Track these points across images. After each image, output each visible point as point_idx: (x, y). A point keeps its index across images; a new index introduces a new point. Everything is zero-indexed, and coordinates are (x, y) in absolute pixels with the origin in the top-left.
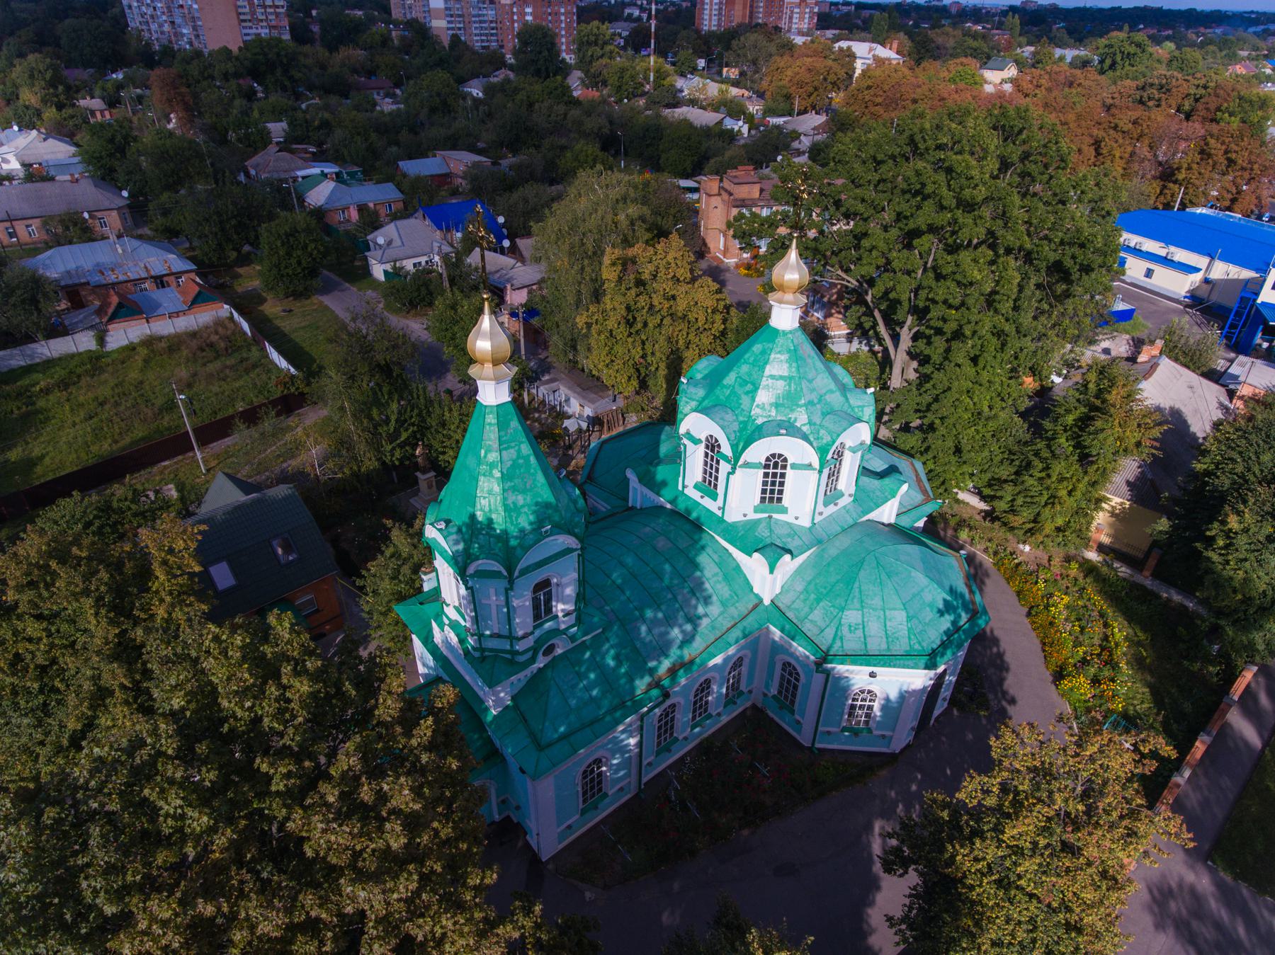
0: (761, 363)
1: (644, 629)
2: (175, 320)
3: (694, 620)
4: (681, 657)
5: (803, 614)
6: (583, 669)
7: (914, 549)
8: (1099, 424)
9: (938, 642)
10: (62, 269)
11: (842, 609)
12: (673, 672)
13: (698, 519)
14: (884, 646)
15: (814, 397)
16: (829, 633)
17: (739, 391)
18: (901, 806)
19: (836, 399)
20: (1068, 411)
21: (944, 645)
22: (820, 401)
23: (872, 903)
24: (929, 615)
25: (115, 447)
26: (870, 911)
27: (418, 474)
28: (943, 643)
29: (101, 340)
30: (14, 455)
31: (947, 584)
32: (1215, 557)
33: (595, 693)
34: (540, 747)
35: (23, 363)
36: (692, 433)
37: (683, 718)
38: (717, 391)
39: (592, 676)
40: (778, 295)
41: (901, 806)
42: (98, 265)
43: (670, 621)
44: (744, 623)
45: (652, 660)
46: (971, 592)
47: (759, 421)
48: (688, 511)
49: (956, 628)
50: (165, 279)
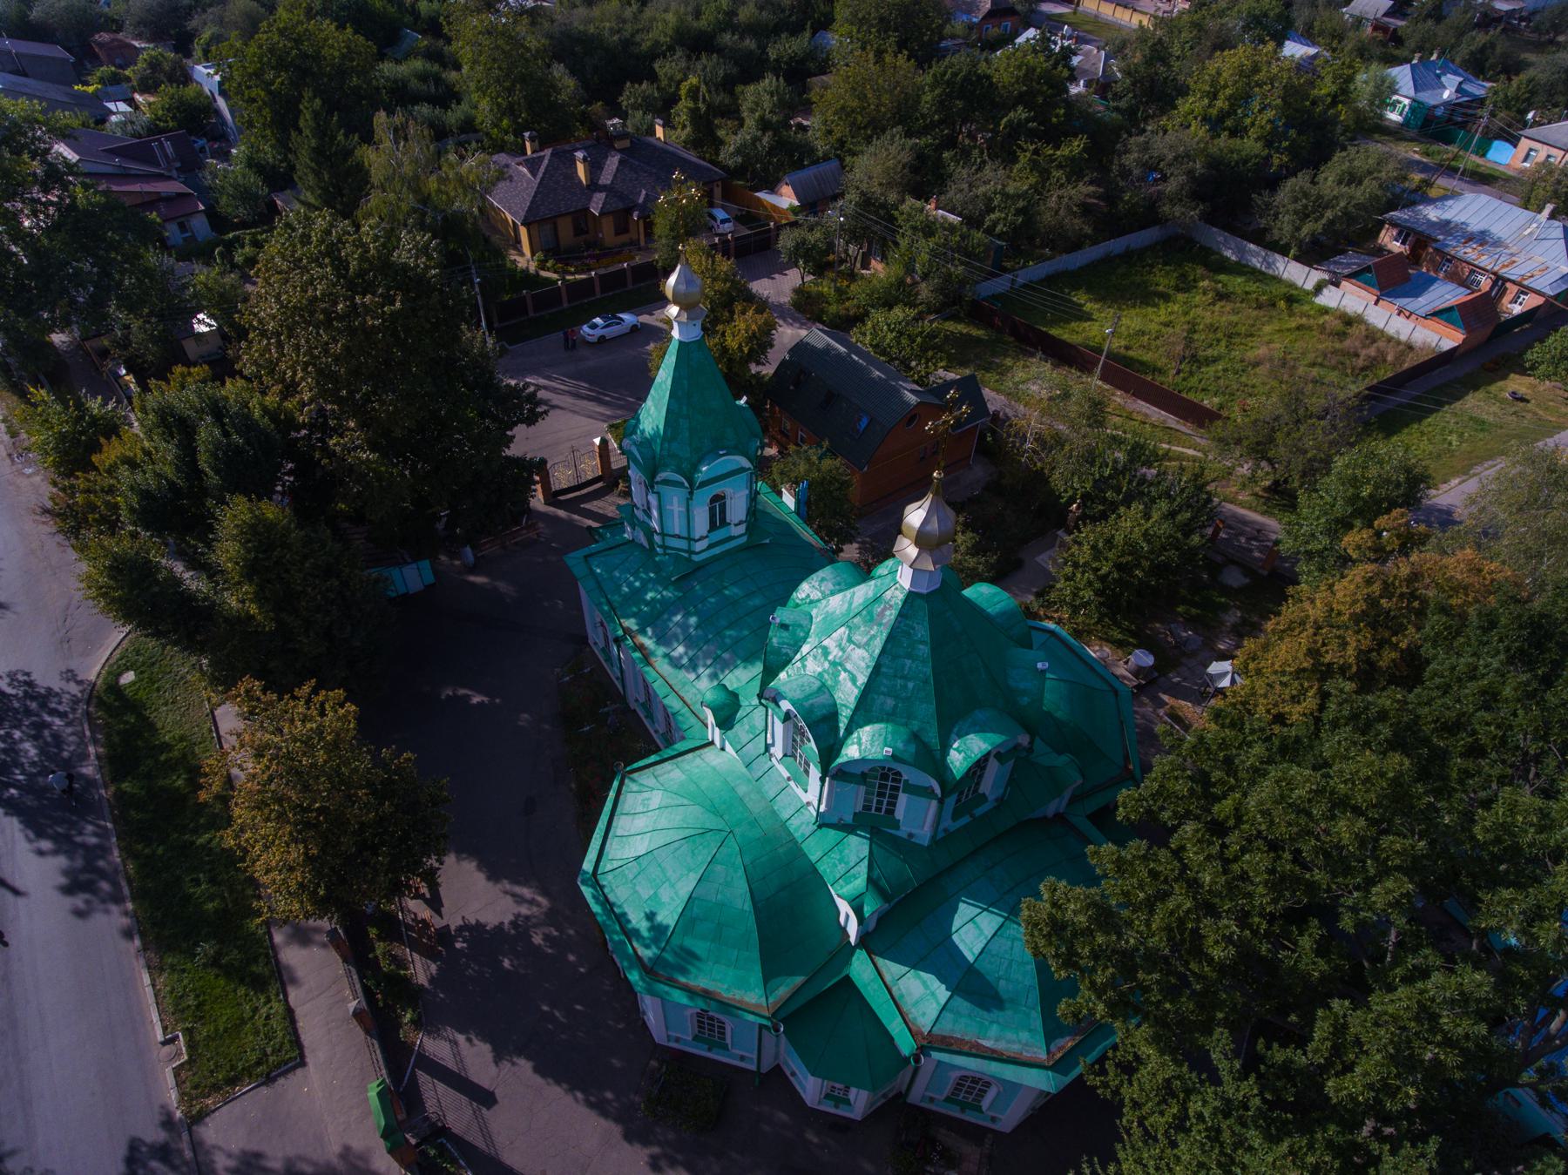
1: (678, 618)
2: (1395, 317)
3: (693, 666)
4: (656, 656)
6: (644, 576)
7: (739, 895)
9: (611, 897)
10: (1447, 216)
12: (641, 648)
14: (619, 833)
15: (835, 653)
18: (556, 933)
19: (847, 695)
21: (607, 904)
22: (833, 664)
23: (479, 868)
24: (645, 892)
25: (1123, 351)
26: (474, 864)
28: (612, 905)
29: (1319, 289)
30: (1089, 307)
31: (699, 947)
33: (626, 589)
34: (586, 557)
35: (1258, 265)
37: (659, 716)
39: (637, 584)
41: (556, 933)
42: (1483, 232)
43: (689, 642)
44: (688, 714)
45: (654, 632)
46: (691, 992)
47: (814, 612)
49: (632, 934)
50: (1508, 285)
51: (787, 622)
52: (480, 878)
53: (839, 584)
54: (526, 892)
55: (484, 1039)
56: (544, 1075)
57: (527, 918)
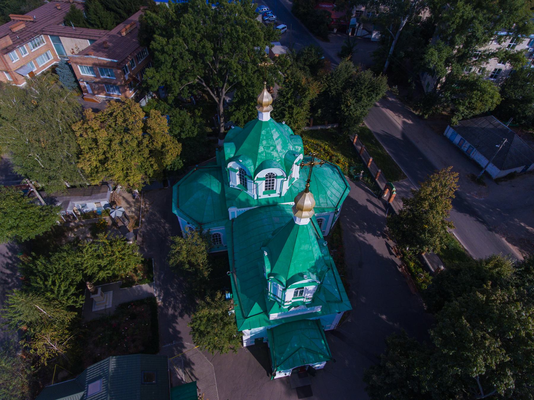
0: (270, 137)
5: (318, 204)
8: (307, 93)
11: (326, 193)
13: (274, 202)
14: (339, 194)
16: (329, 202)
17: (269, 152)
20: (287, 94)
27: (92, 296)
32: (346, 114)
36: (259, 177)
38: (259, 157)
40: (265, 108)
47: (283, 157)
48: (268, 202)
51: (293, 156)
52: (375, 247)
53: (271, 162)
54: (361, 239)
55: (369, 211)
56: (355, 200)
57: (361, 232)
